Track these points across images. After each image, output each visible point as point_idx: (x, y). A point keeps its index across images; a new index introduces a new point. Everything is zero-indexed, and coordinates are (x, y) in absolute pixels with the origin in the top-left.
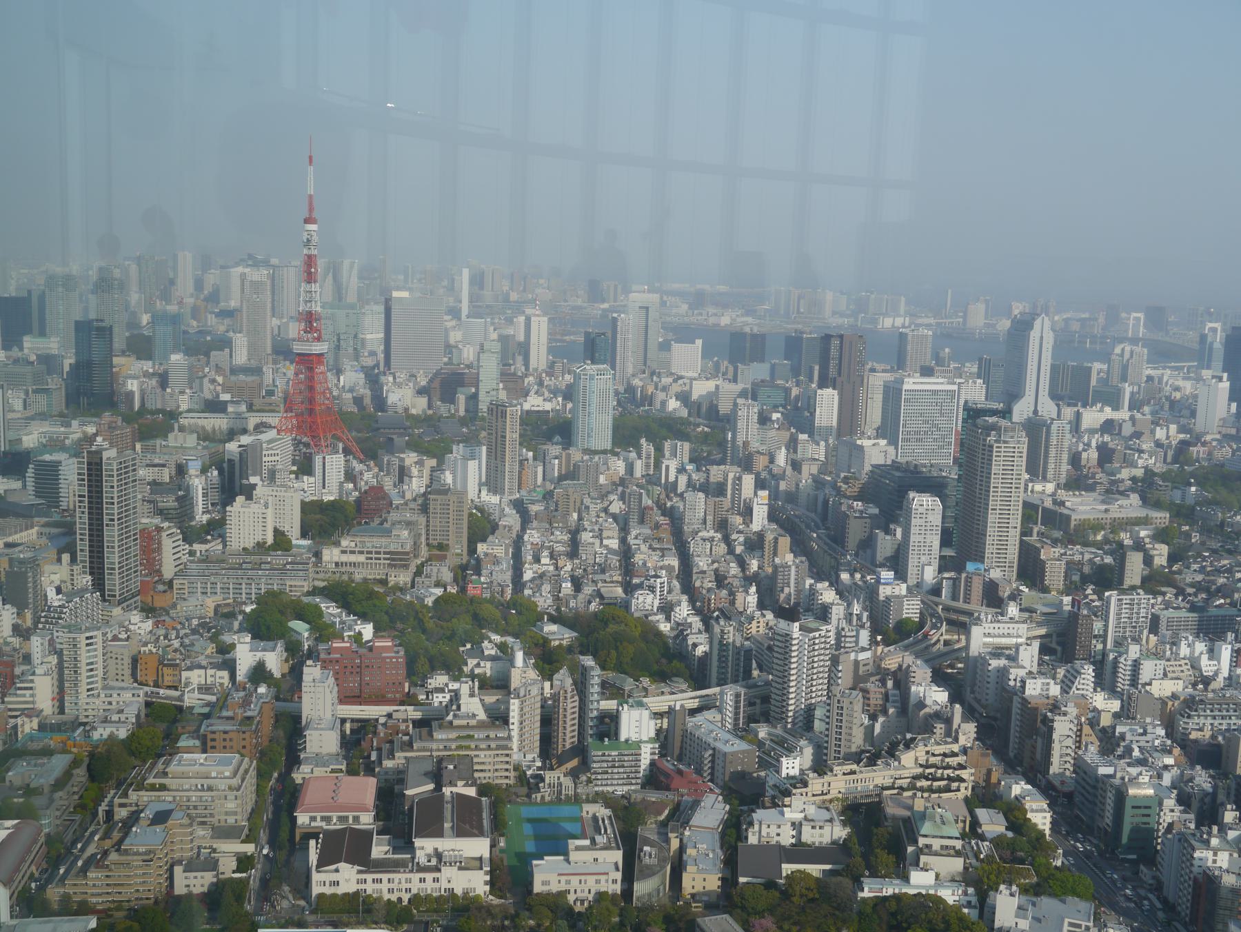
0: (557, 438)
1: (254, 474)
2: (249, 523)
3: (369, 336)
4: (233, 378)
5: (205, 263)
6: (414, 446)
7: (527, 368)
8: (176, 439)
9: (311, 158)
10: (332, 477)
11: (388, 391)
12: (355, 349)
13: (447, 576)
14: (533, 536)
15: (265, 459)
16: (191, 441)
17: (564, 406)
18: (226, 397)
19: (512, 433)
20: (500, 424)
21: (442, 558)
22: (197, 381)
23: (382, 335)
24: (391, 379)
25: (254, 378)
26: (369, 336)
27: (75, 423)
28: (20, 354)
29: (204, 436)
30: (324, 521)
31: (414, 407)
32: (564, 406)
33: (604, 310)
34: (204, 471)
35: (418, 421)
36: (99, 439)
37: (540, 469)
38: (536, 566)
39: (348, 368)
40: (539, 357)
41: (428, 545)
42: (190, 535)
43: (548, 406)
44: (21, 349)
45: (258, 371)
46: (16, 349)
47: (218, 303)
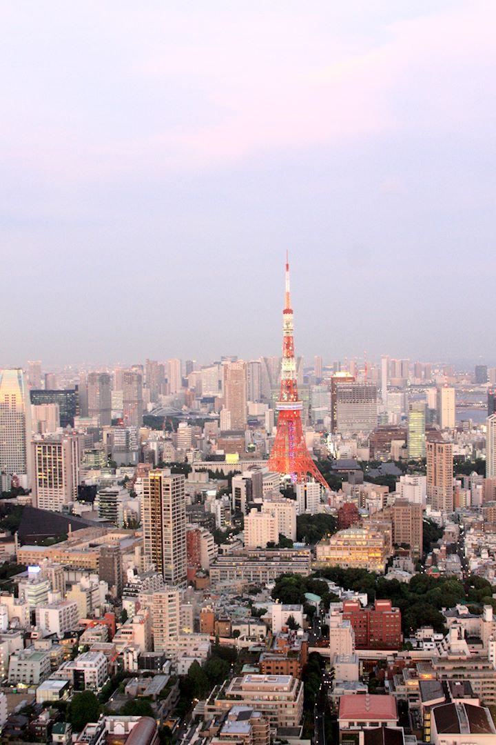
0: (474, 474)
1: (257, 497)
2: (261, 528)
3: (317, 409)
4: (224, 439)
5: (190, 367)
6: (368, 479)
7: (441, 427)
8: (194, 477)
9: (287, 265)
10: (315, 496)
12: (310, 417)
13: (411, 566)
14: (471, 539)
15: (264, 487)
16: (205, 476)
17: (474, 452)
18: (221, 452)
19: (447, 466)
20: (438, 457)
21: (405, 554)
22: (198, 442)
25: (239, 439)
26: (317, 409)
27: (118, 471)
28: (72, 430)
29: (213, 475)
30: (314, 529)
32: (474, 452)
33: (489, 388)
34: (218, 497)
35: (363, 464)
36: (139, 479)
37: (469, 492)
38: (479, 559)
39: (306, 430)
40: (448, 419)
41: (393, 545)
42: (220, 538)
43: (463, 452)
44: (73, 427)
45: (242, 433)
46: (69, 426)
47: (201, 393)
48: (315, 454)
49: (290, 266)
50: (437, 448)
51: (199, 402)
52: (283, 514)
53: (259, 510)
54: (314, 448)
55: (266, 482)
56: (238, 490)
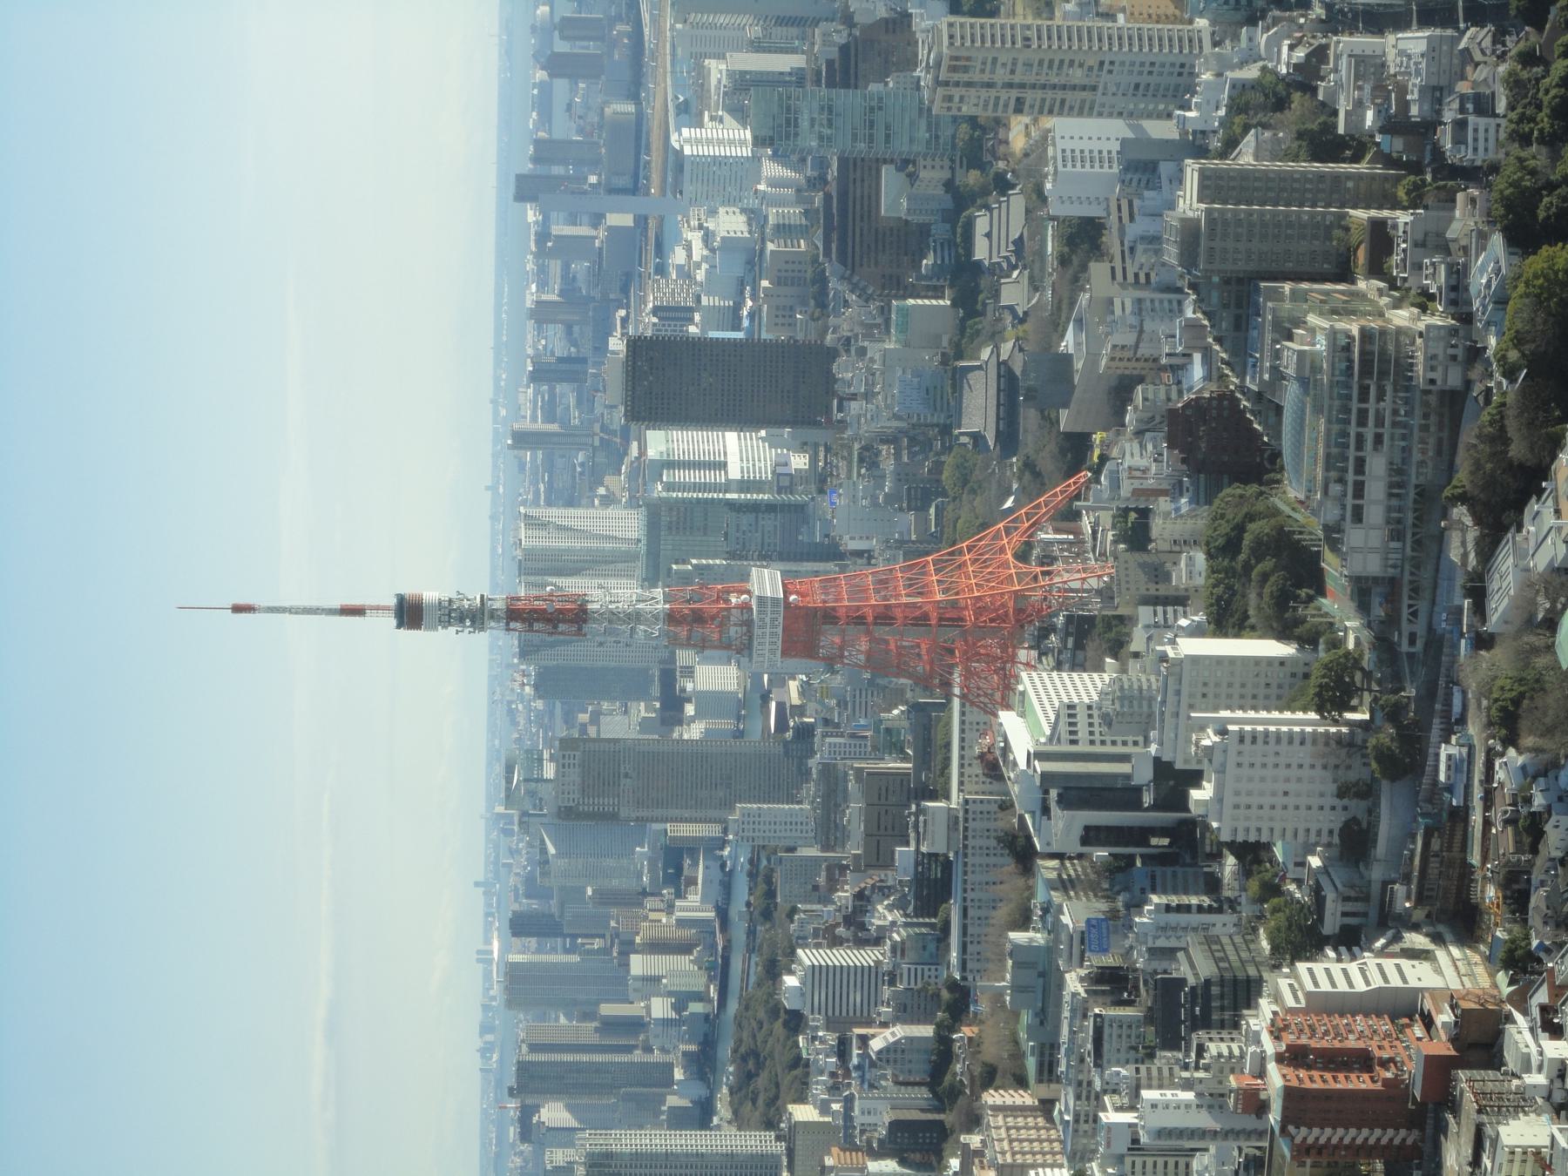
11: (896, 417)
21: (1381, 236)
23: (731, 437)
24: (854, 407)
31: (939, 337)
48: (925, 508)
49: (242, 601)
50: (956, 77)
51: (678, 903)
52: (1210, 691)
53: (1195, 778)
54: (901, 509)
55: (1063, 728)
56: (1092, 836)
